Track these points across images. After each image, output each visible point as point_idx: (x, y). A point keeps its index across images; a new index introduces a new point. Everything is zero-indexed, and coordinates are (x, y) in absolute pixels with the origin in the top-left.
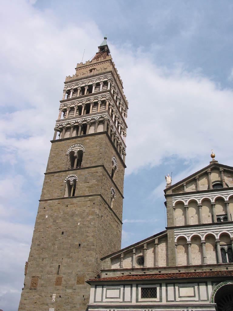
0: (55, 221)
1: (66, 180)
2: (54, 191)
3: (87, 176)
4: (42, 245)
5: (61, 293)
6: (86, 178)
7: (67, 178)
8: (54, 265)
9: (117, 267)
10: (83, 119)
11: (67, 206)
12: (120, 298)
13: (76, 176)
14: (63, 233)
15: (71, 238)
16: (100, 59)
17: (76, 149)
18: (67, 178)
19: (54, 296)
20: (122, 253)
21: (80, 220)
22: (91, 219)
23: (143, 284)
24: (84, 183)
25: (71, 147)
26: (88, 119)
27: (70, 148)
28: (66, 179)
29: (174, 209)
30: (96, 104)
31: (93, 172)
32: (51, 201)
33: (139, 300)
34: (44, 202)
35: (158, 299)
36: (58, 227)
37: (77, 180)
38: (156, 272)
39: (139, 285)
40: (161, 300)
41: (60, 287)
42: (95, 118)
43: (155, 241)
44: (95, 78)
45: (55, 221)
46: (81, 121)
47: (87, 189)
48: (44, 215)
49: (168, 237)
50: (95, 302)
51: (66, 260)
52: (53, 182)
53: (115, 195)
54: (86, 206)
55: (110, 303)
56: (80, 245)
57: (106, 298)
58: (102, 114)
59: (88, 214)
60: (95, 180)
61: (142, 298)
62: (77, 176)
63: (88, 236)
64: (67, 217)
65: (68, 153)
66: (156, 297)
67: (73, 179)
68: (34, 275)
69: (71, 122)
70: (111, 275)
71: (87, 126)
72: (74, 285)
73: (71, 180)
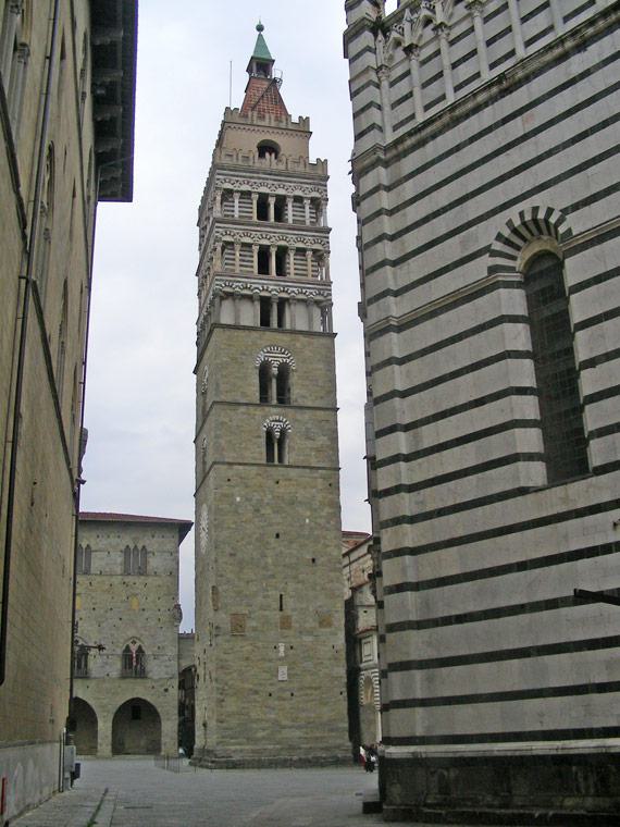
0: (258, 511)
3: (309, 426)
4: (239, 555)
5: (294, 641)
6: (307, 430)
8: (270, 593)
14: (278, 536)
15: (294, 546)
17: (276, 361)
19: (282, 649)
21: (308, 513)
30: (301, 251)
32: (241, 467)
34: (225, 467)
41: (291, 632)
51: (291, 586)
54: (315, 487)
56: (314, 560)
60: (326, 438)
63: (328, 546)
69: (254, 286)
72: (315, 628)
73: (277, 428)
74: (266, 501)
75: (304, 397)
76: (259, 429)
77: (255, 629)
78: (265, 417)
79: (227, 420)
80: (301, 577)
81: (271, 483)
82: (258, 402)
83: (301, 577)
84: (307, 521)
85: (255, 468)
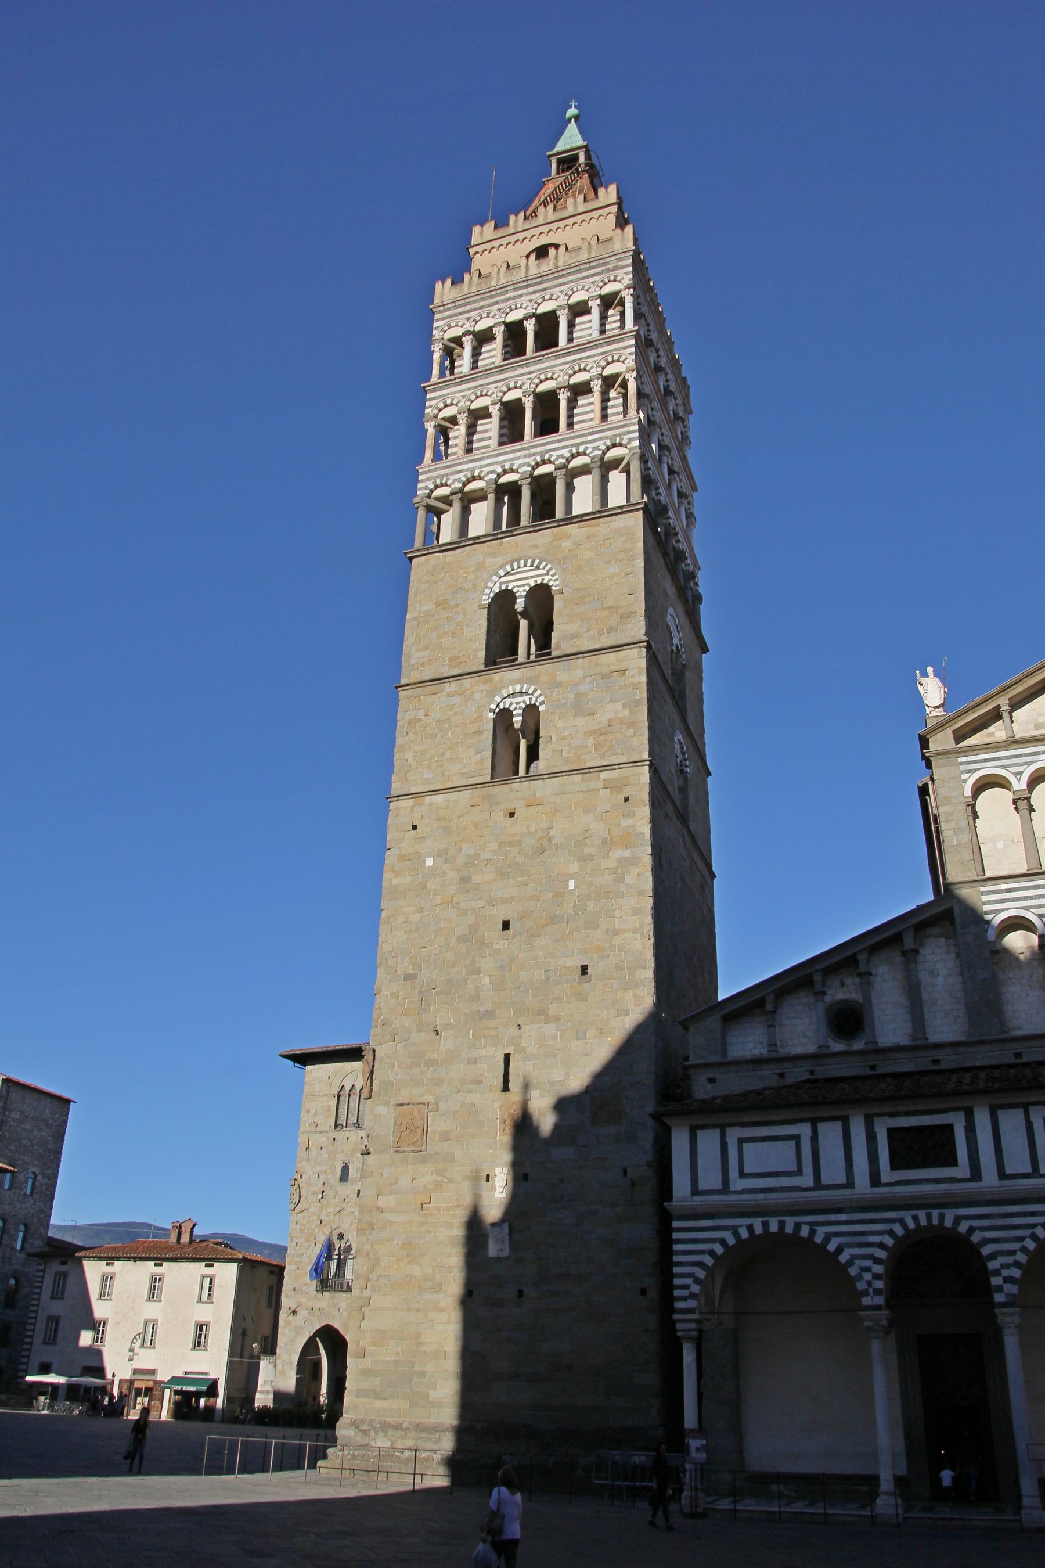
0: (465, 880)
1: (491, 710)
2: (448, 755)
3: (582, 689)
7: (498, 699)
8: (483, 1052)
9: (750, 1050)
10: (534, 455)
11: (512, 815)
12: (799, 1172)
13: (535, 691)
14: (506, 925)
16: (570, 201)
18: (498, 699)
20: (768, 994)
21: (574, 867)
22: (620, 860)
23: (892, 1115)
24: (576, 715)
25: (496, 574)
26: (558, 457)
27: (495, 578)
28: (493, 706)
29: (968, 805)
31: (606, 670)
32: (439, 798)
33: (884, 1179)
35: (962, 1170)
36: (481, 903)
37: (542, 708)
38: (921, 1062)
39: (876, 1120)
40: (976, 1174)
42: (587, 448)
43: (905, 940)
44: (564, 284)
45: (465, 880)
46: (528, 465)
47: (591, 741)
48: (419, 858)
49: (958, 920)
50: (695, 1192)
52: (439, 721)
53: (687, 763)
55: (761, 1196)
56: (584, 970)
57: (742, 1175)
58: (617, 432)
59: (607, 844)
60: (619, 706)
61: (894, 1166)
62: (539, 692)
63: (616, 932)
64: (519, 859)
65: (486, 600)
66: (953, 1162)
67: (524, 702)
68: (404, 1096)
69: (485, 470)
70: (732, 1084)
71: (555, 483)
73: (517, 707)
74: (485, 855)
75: (573, 636)
76: (480, 718)
77: (445, 1137)
78: (491, 694)
79: (421, 714)
80: (552, 1010)
81: (500, 817)
82: (482, 668)
83: (552, 1010)
84: (571, 884)
85: (466, 794)
